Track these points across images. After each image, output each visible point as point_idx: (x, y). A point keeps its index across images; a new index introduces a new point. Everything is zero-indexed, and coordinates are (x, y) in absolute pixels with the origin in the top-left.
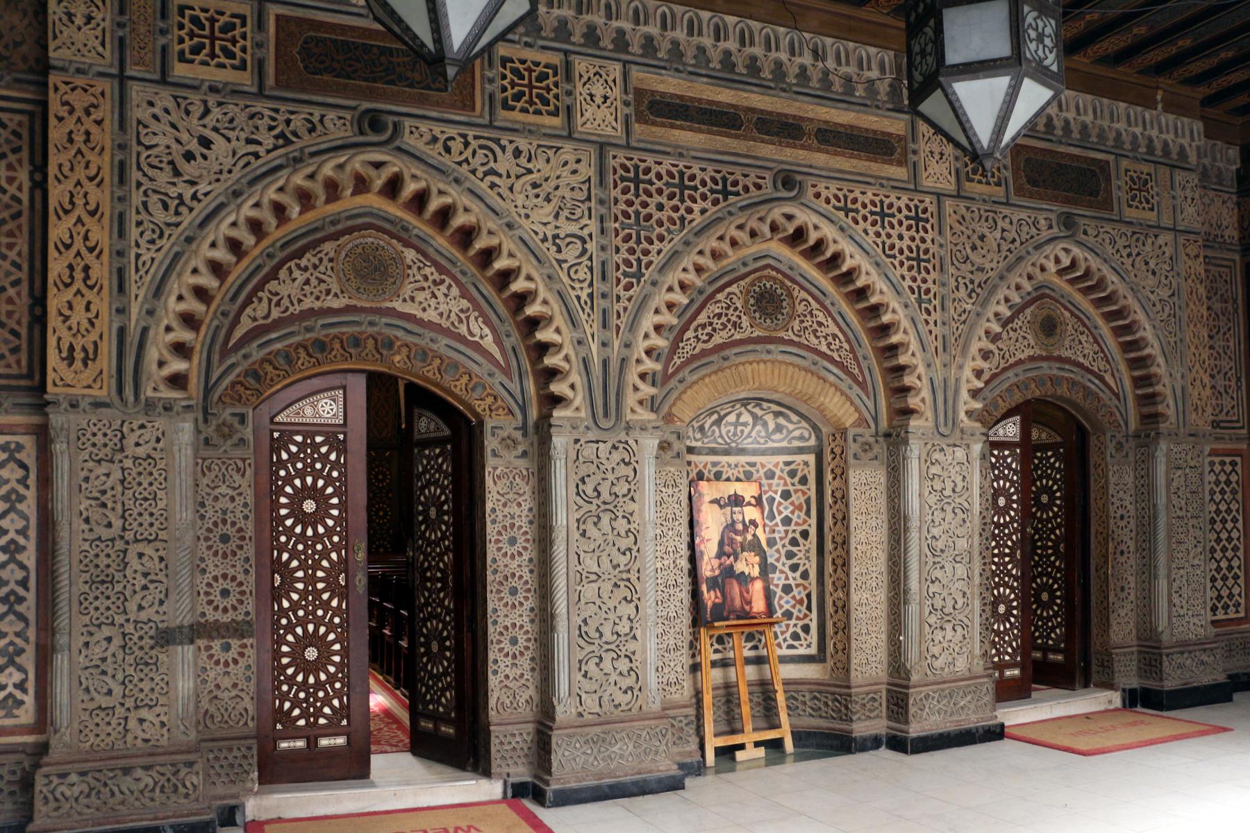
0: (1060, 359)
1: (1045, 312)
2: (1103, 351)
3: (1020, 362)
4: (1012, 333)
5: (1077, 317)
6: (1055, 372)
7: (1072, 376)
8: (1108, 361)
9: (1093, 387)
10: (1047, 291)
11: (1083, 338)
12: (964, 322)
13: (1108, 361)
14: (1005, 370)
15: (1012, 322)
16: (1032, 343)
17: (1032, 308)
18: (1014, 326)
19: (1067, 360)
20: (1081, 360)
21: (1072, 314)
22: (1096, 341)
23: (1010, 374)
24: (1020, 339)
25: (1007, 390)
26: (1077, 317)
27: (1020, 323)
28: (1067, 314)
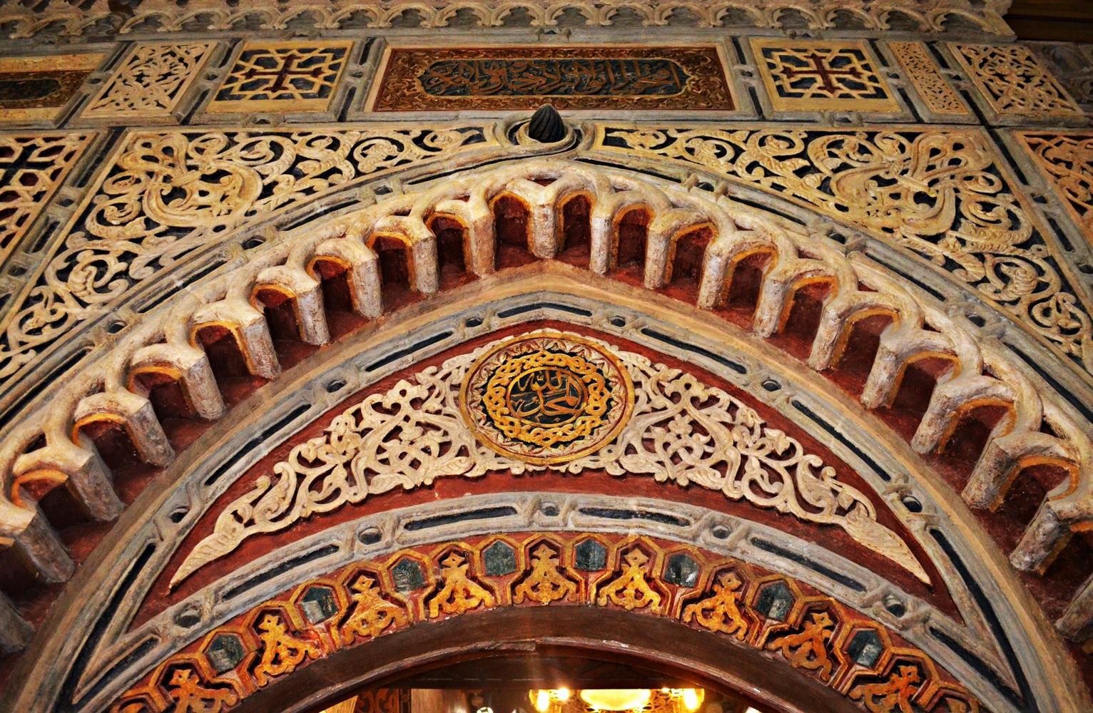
0: (593, 479)
1: (534, 364)
2: (813, 447)
3: (399, 495)
4: (371, 418)
5: (688, 367)
6: (575, 521)
7: (661, 529)
8: (846, 474)
9: (782, 565)
10: (553, 314)
11: (712, 419)
12: (39, 348)
13: (846, 474)
14: (311, 522)
15: (383, 392)
16: (459, 434)
17: (479, 353)
18: (392, 397)
19: (628, 482)
20: (710, 479)
21: (656, 357)
22: (772, 418)
23: (338, 534)
24: (409, 432)
25: (310, 593)
26: (672, 362)
27: (413, 392)
28: (629, 358)
